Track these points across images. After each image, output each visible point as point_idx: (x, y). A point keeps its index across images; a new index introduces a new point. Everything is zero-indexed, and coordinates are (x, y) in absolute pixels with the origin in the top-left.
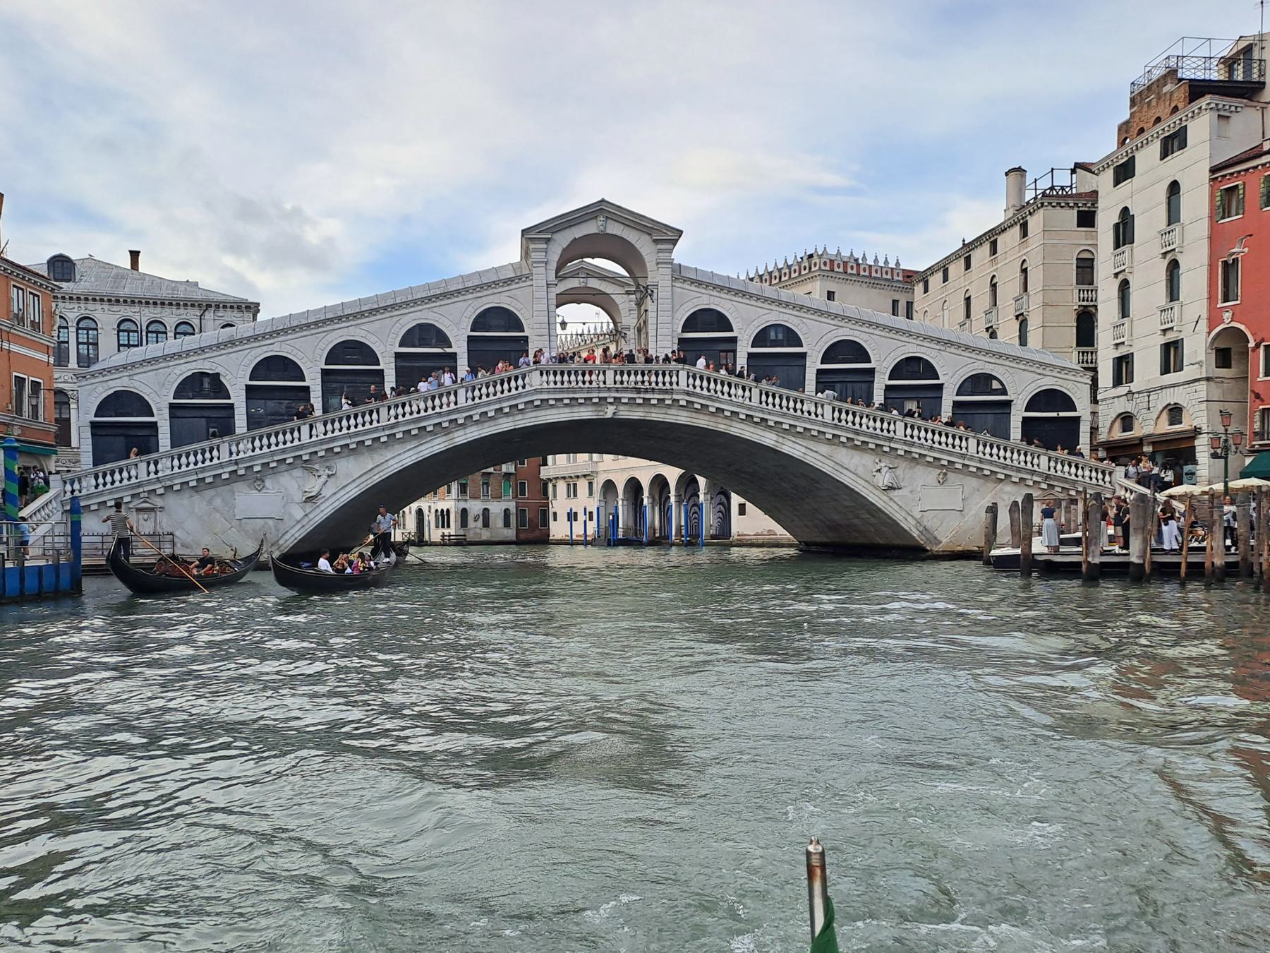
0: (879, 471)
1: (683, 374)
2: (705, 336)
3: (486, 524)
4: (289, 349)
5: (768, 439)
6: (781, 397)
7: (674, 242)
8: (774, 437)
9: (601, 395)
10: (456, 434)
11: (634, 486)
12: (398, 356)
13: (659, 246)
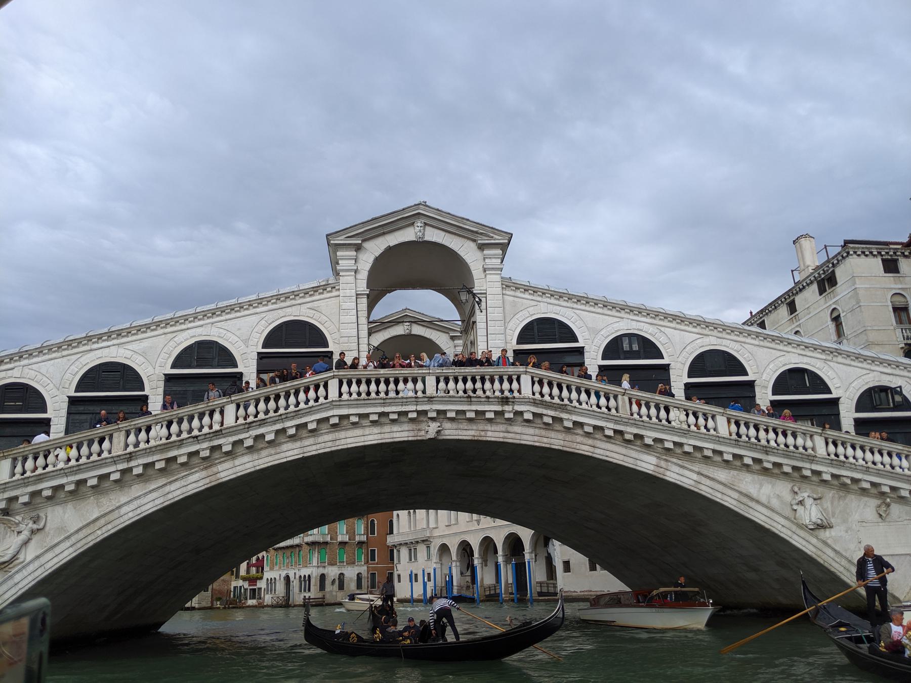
0: (801, 503)
1: (526, 380)
2: (548, 344)
3: (341, 587)
4: (32, 374)
5: (647, 463)
6: (657, 407)
7: (504, 247)
8: (652, 460)
9: (420, 408)
10: (220, 467)
11: (465, 549)
12: (169, 378)
13: (486, 252)
